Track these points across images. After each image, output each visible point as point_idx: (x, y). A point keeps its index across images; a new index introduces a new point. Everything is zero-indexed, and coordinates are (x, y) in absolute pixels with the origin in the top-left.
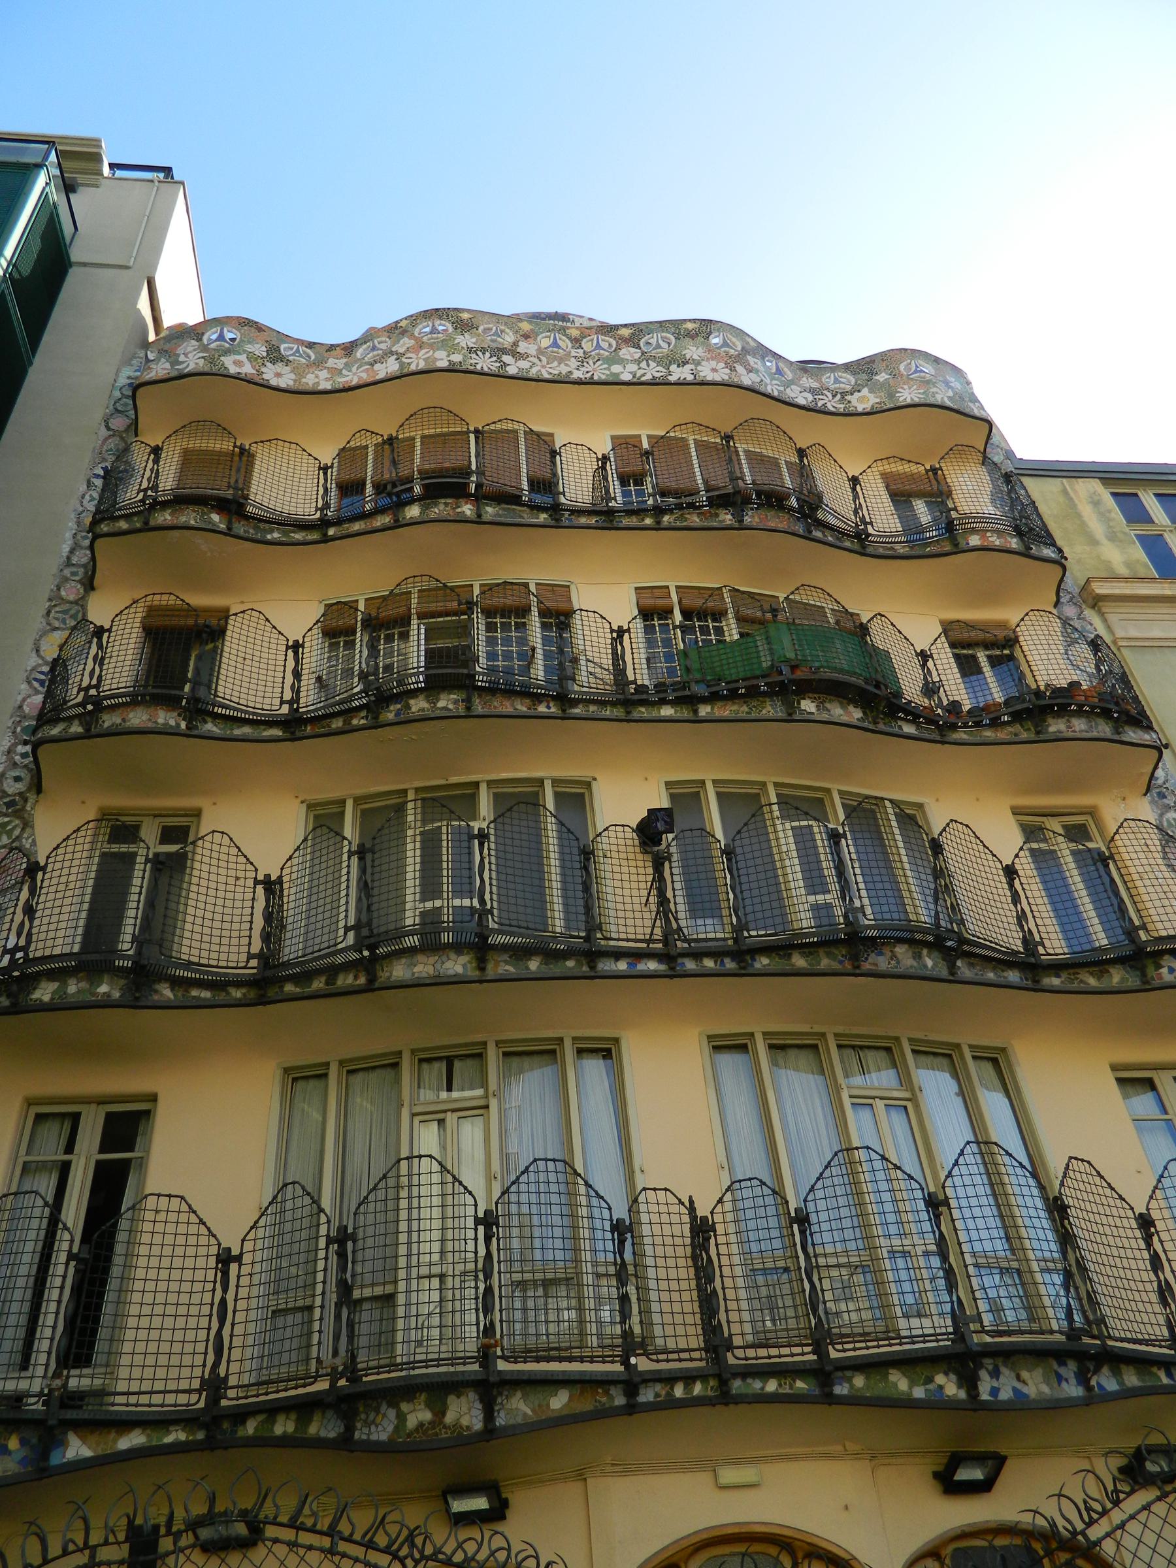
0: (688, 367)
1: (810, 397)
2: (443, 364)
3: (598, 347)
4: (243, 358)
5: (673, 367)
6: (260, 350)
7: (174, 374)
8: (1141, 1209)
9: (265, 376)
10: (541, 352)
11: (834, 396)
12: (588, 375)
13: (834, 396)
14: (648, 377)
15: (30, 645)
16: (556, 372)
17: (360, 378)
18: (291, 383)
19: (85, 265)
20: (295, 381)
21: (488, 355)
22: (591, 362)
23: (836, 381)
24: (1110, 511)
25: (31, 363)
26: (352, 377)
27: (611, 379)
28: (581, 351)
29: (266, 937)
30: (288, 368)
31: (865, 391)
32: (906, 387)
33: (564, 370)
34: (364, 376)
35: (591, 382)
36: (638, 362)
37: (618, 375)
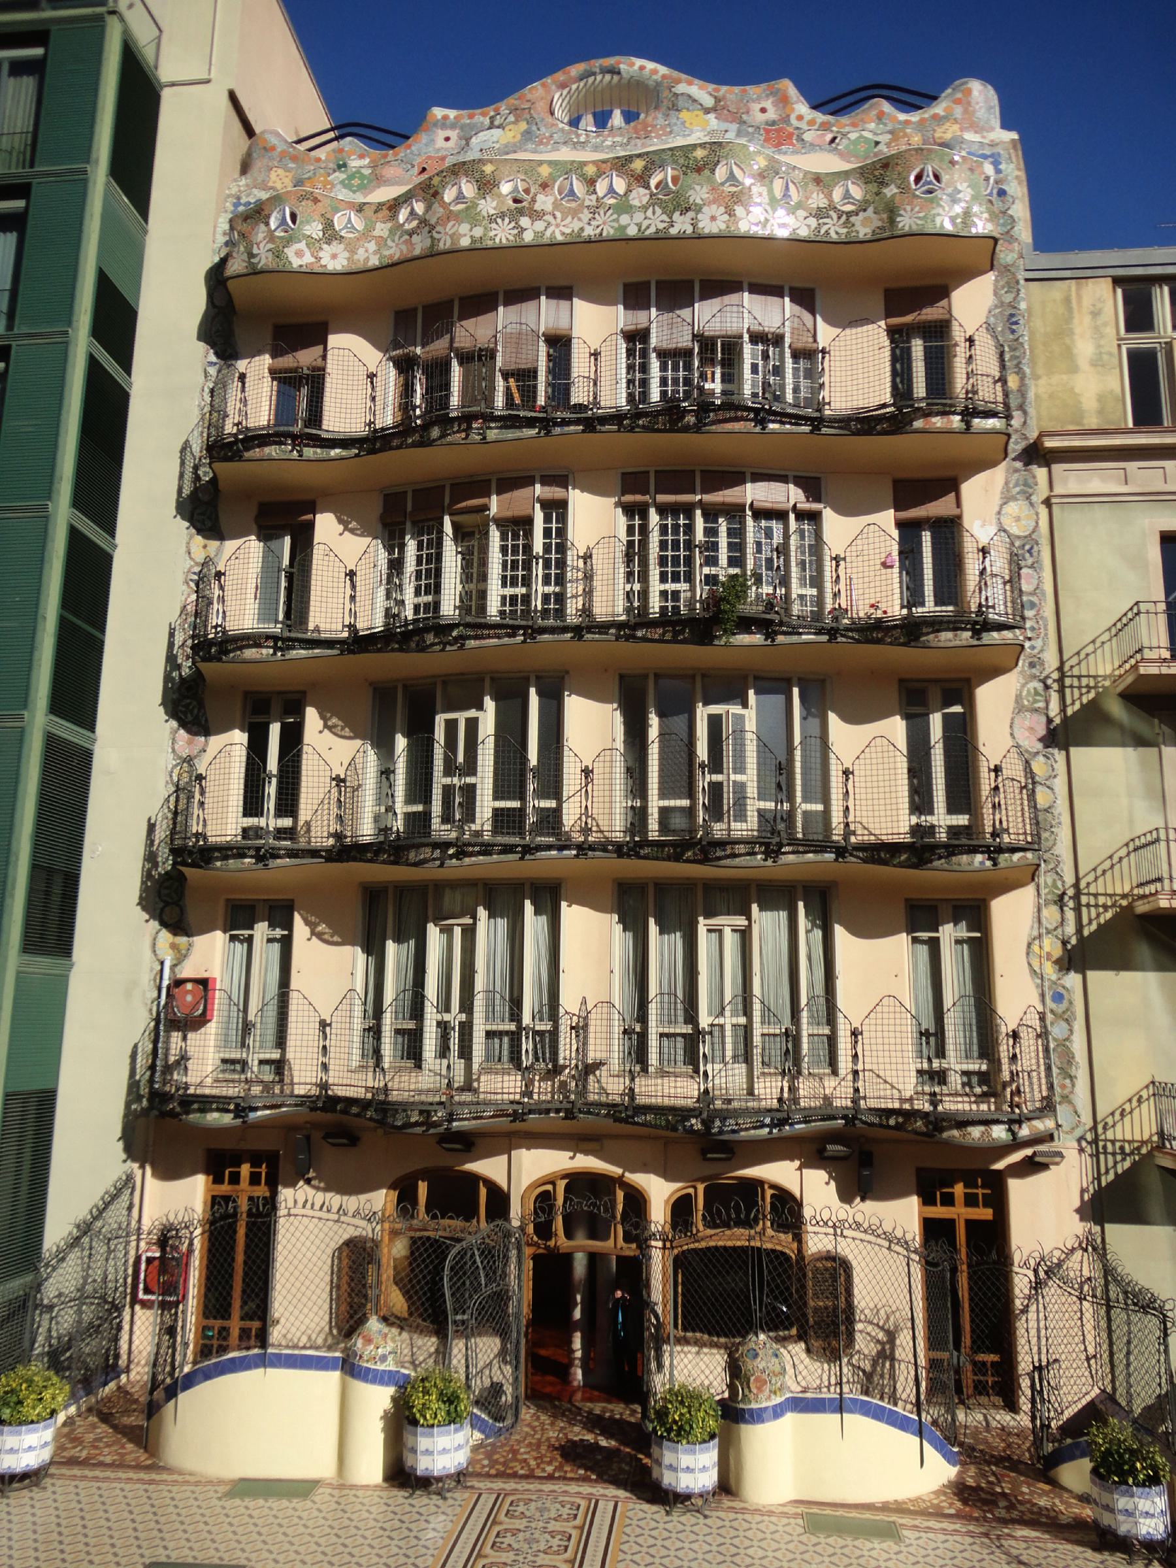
0: (691, 214)
1: (813, 222)
2: (465, 242)
3: (611, 190)
4: (302, 246)
6: (314, 229)
8: (856, 1024)
9: (323, 262)
10: (556, 205)
14: (652, 230)
15: (184, 549)
16: (568, 231)
18: (345, 263)
19: (173, 84)
21: (507, 220)
23: (847, 195)
24: (1105, 324)
25: (146, 232)
27: (618, 235)
28: (594, 197)
29: (340, 818)
30: (342, 246)
31: (871, 210)
32: (908, 208)
33: (576, 225)
36: (645, 208)
37: (625, 227)
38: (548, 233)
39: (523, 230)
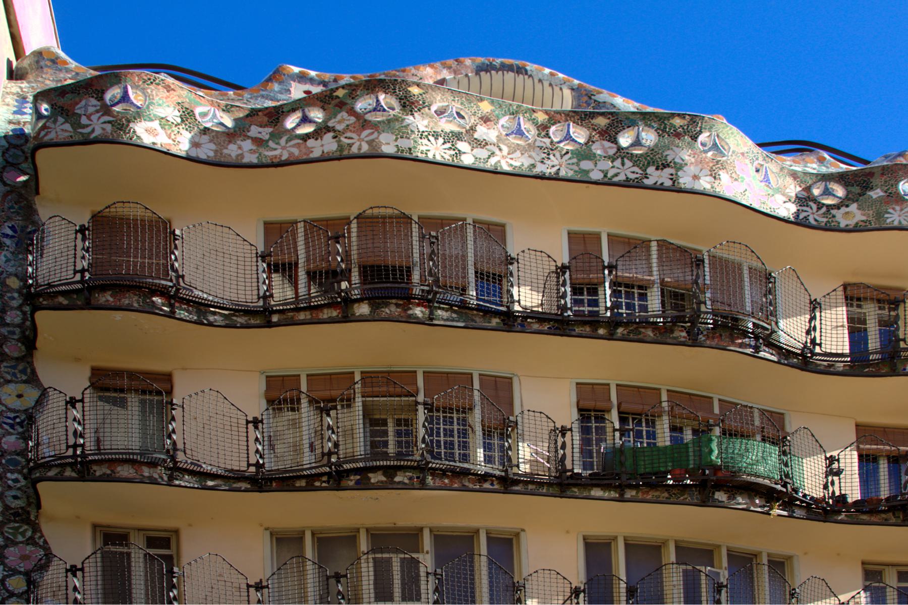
0: (668, 171)
5: (651, 170)
7: (77, 138)
11: (819, 209)
12: (554, 170)
13: (819, 209)
14: (621, 177)
16: (518, 164)
17: (291, 154)
18: (212, 154)
20: (216, 151)
22: (558, 155)
26: (279, 151)
27: (578, 177)
32: (898, 208)
34: (296, 152)
35: (556, 178)
37: (587, 172)
38: (493, 161)
39: (460, 152)
